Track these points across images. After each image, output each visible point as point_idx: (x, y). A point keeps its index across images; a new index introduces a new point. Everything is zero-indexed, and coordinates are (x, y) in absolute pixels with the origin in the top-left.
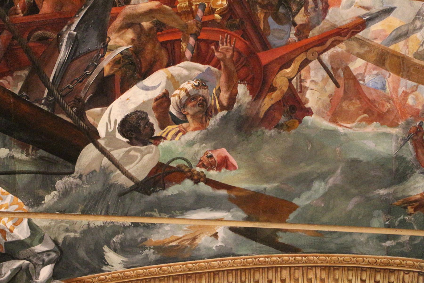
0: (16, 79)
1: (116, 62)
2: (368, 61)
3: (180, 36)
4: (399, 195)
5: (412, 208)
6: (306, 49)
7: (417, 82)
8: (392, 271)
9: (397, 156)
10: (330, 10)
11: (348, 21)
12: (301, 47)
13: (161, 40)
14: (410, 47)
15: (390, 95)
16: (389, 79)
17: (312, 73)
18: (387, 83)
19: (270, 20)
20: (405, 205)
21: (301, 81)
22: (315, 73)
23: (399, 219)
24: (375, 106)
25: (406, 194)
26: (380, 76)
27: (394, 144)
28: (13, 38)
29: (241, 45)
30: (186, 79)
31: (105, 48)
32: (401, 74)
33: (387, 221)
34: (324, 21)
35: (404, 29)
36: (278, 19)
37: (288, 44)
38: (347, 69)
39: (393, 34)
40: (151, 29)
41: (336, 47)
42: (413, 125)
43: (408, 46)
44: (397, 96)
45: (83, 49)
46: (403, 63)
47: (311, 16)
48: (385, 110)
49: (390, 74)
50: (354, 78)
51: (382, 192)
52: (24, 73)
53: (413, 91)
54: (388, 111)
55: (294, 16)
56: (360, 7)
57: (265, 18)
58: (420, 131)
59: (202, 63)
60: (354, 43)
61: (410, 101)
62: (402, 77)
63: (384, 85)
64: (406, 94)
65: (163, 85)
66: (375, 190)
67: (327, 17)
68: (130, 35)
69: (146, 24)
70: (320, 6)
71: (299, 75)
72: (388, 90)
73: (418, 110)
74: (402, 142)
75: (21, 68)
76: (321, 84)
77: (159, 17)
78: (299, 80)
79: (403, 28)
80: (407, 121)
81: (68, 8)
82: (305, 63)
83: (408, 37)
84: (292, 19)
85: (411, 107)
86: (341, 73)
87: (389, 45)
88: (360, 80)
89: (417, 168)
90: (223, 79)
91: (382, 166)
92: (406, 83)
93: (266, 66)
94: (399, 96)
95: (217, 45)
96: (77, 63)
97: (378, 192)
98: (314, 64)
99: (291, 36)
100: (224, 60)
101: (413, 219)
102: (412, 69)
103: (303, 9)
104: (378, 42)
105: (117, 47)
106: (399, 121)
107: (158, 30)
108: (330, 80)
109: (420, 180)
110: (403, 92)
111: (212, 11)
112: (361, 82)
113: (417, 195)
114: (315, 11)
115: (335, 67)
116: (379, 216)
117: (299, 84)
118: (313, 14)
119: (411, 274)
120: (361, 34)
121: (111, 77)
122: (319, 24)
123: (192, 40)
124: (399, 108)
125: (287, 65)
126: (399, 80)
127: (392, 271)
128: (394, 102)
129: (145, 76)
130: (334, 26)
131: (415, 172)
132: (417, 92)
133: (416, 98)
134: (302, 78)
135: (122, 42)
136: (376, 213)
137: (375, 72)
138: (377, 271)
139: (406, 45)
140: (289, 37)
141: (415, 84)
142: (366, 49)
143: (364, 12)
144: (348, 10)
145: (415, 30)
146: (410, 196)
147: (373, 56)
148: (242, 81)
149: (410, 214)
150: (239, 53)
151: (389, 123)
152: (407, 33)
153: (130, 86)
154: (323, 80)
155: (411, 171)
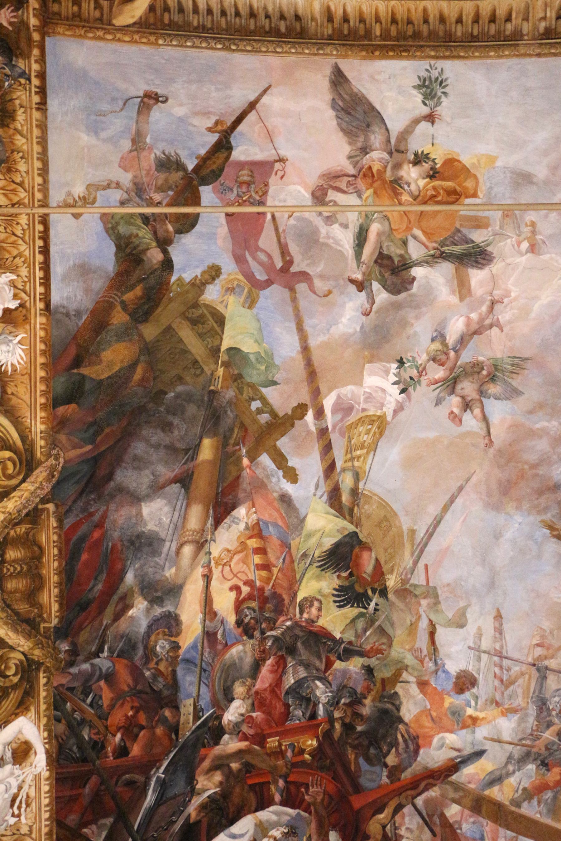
0: (100, 828)
1: (203, 807)
2: (464, 807)
3: (270, 779)
6: (399, 792)
10: (421, 751)
11: (440, 764)
12: (394, 791)
13: (250, 782)
14: (505, 793)
17: (407, 819)
19: (361, 761)
21: (396, 828)
22: (410, 820)
28: (101, 784)
29: (331, 788)
30: (275, 825)
31: (193, 792)
32: (499, 822)
34: (417, 763)
35: (498, 773)
36: (368, 760)
37: (380, 787)
38: (442, 816)
39: (487, 777)
40: (240, 770)
41: (430, 791)
45: (170, 793)
46: (500, 810)
47: (403, 757)
49: (487, 823)
50: (451, 826)
52: (109, 821)
55: (385, 757)
56: (452, 748)
57: (356, 758)
59: (293, 807)
60: (448, 787)
62: (500, 825)
63: (483, 835)
65: (251, 832)
67: (419, 759)
68: (218, 777)
69: (235, 766)
70: (411, 747)
71: (392, 821)
75: (106, 816)
76: (416, 833)
77: (248, 758)
78: (393, 828)
81: (157, 750)
82: (399, 808)
83: (502, 782)
84: (383, 760)
86: (437, 820)
87: (483, 790)
88: (457, 829)
90: (313, 825)
92: (505, 833)
93: (359, 811)
95: (307, 787)
96: (163, 809)
98: (408, 809)
99: (383, 778)
100: (314, 804)
103: (394, 749)
104: (472, 786)
105: (205, 791)
107: (248, 772)
108: (426, 829)
111: (302, 751)
112: (459, 831)
114: (406, 752)
115: (430, 813)
117: (393, 831)
118: (404, 756)
120: (454, 777)
121: (198, 823)
122: (411, 766)
123: (281, 783)
125: (380, 810)
126: (498, 830)
129: (232, 822)
130: (426, 768)
134: (397, 825)
135: (210, 785)
137: (472, 820)
139: (501, 790)
140: (381, 780)
141: (514, 834)
142: (461, 794)
143: (455, 754)
144: (439, 752)
145: (508, 775)
147: (468, 801)
148: (334, 827)
150: (330, 797)
153: (216, 834)
154: (419, 828)
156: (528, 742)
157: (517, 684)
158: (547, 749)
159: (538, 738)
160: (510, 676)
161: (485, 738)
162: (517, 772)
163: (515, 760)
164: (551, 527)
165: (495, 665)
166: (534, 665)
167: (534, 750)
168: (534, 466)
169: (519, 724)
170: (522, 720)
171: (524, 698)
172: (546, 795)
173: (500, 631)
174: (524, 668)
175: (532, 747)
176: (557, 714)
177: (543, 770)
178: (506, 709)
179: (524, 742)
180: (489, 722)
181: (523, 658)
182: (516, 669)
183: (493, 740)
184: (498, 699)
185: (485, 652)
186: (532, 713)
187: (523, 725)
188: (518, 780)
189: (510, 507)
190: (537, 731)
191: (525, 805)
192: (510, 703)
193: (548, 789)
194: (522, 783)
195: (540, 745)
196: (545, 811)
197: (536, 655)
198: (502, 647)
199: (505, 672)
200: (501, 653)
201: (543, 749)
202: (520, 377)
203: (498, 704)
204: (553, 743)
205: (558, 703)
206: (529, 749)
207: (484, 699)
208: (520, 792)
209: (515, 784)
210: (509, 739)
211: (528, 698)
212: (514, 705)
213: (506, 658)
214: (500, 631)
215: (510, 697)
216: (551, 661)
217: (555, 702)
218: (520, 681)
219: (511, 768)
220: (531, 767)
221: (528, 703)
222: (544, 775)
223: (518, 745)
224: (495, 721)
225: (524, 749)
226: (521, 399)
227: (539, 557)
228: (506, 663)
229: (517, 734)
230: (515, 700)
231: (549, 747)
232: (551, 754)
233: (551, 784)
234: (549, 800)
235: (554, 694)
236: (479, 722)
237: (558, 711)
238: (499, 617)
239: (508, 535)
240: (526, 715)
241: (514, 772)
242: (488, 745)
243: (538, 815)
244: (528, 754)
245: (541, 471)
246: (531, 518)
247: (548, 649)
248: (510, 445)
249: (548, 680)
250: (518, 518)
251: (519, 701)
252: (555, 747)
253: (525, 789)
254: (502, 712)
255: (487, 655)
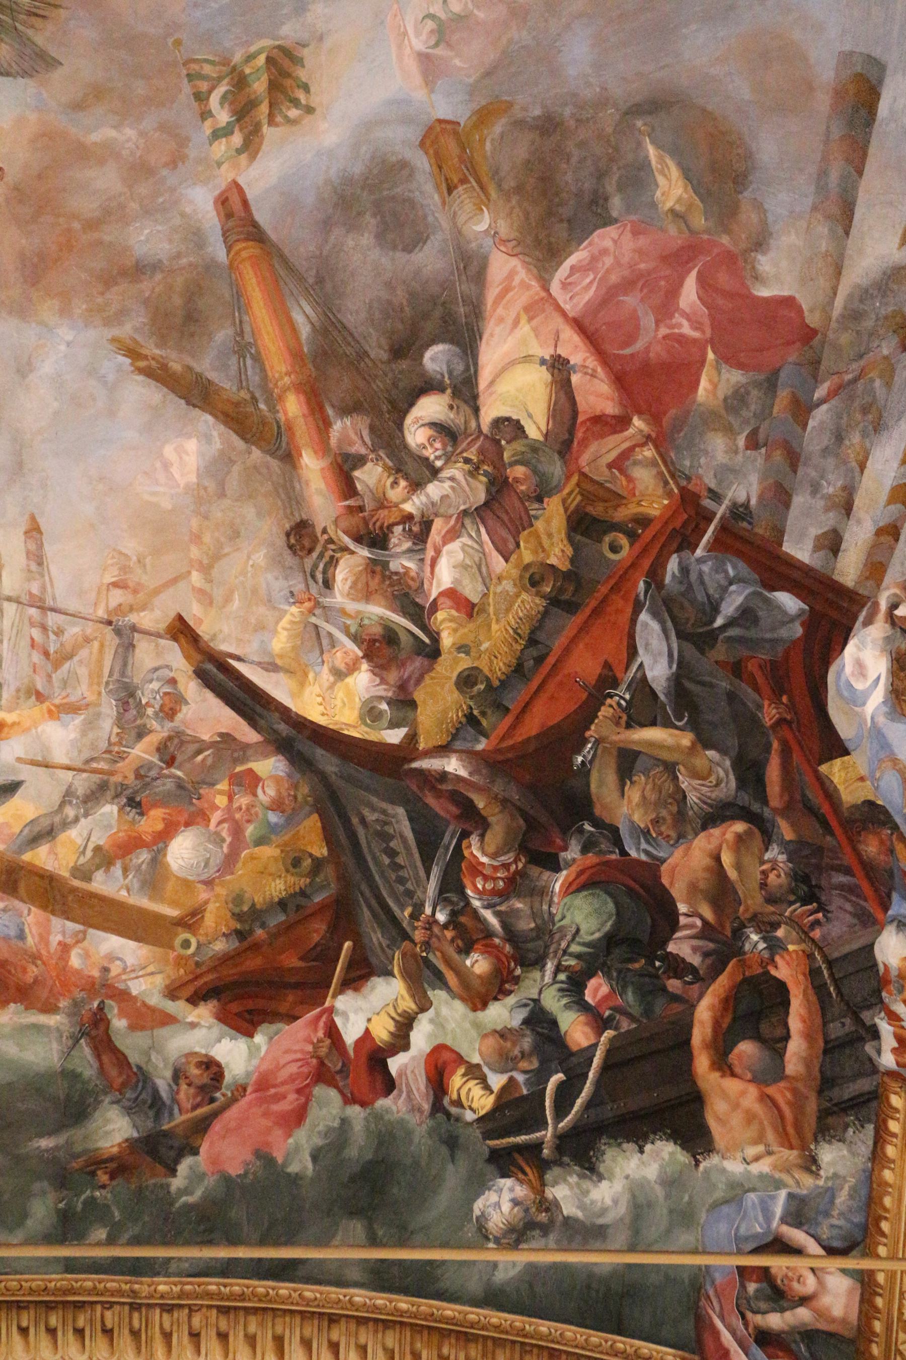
4: (78, 1148)
5: (106, 1173)
7: (83, 924)
8: (79, 1306)
9: (63, 1070)
14: (60, 856)
15: (34, 949)
16: (30, 919)
18: (26, 926)
20: (93, 1168)
23: (83, 1197)
24: (9, 972)
25: (91, 1146)
26: (10, 913)
27: (55, 1045)
33: (60, 1202)
35: (45, 823)
39: (26, 831)
42: (87, 1007)
43: (56, 854)
44: (49, 952)
46: (52, 888)
48: (29, 978)
49: (30, 910)
51: (45, 1143)
53: (78, 942)
54: (36, 981)
58: (102, 1020)
61: (75, 961)
62: (53, 913)
63: (22, 931)
64: (65, 948)
66: (30, 1140)
72: (30, 941)
73: (93, 977)
74: (70, 1042)
79: (42, 820)
80: (73, 1000)
83: (54, 838)
85: (77, 972)
89: (106, 1094)
91: (37, 1090)
92: (64, 926)
94: (52, 950)
97: (37, 1145)
101: (109, 1196)
102: (70, 899)
106: (58, 1000)
109: (114, 1116)
110: (60, 943)
113: (112, 1146)
116: (44, 1193)
119: (117, 1308)
124: (54, 974)
126: (49, 920)
127: (79, 1306)
128: (44, 963)
131: (102, 1101)
132: (85, 944)
133: (87, 955)
136: (37, 1186)
138: (49, 1306)
139: (52, 852)
145: (66, 825)
146: (97, 1149)
149: (104, 1187)
151: (39, 1005)
152: (52, 830)
155: (95, 1099)
156: (102, 765)
157: (76, 659)
158: (138, 776)
159: (121, 757)
160: (62, 645)
161: (19, 760)
162: (83, 820)
163: (78, 798)
164: (133, 352)
165: (32, 624)
166: (110, 623)
167: (117, 778)
168: (92, 225)
169: (84, 733)
170: (90, 725)
171: (91, 685)
172: (138, 858)
173: (38, 558)
174: (90, 629)
175: (111, 773)
176: (156, 714)
177: (131, 815)
178: (57, 706)
179: (95, 765)
180: (27, 730)
181: (87, 611)
182: (73, 631)
183: (34, 763)
184: (40, 687)
185: (9, 599)
186: (108, 711)
187: (91, 735)
188: (85, 835)
189: (48, 310)
190: (120, 743)
191: (99, 876)
192: (64, 694)
193: (141, 847)
194: (93, 839)
195: (125, 772)
196: (136, 885)
197: (113, 603)
198: (43, 588)
199: (52, 637)
200: (42, 600)
201: (132, 776)
202: (50, 27)
203: (40, 697)
204: (150, 766)
205: (158, 692)
206: (105, 777)
207: (13, 688)
208: (89, 854)
209: (80, 841)
210: (65, 761)
211: (99, 684)
212: (72, 699)
213: (53, 610)
214: (38, 558)
215: (65, 683)
216: (142, 614)
217: (152, 691)
218: (84, 653)
219: (70, 812)
220: (109, 810)
221: (100, 694)
222: (133, 822)
223: (84, 771)
224: (36, 728)
225: (96, 778)
226: (57, 75)
227: (111, 413)
228: (52, 619)
229: (80, 751)
230: (75, 688)
231: (142, 773)
232: (146, 785)
233: (148, 838)
234: (144, 867)
235: (150, 676)
236: (6, 730)
237: (157, 707)
238: (34, 530)
239: (47, 367)
240: (98, 715)
241: (76, 820)
242: (25, 773)
243: (124, 893)
244: (103, 787)
245: (109, 234)
246: (92, 334)
247: (135, 592)
248: (39, 177)
249: (137, 651)
250: (65, 333)
251: (83, 691)
252: (153, 773)
253: (98, 849)
254: (50, 712)
255: (14, 606)
